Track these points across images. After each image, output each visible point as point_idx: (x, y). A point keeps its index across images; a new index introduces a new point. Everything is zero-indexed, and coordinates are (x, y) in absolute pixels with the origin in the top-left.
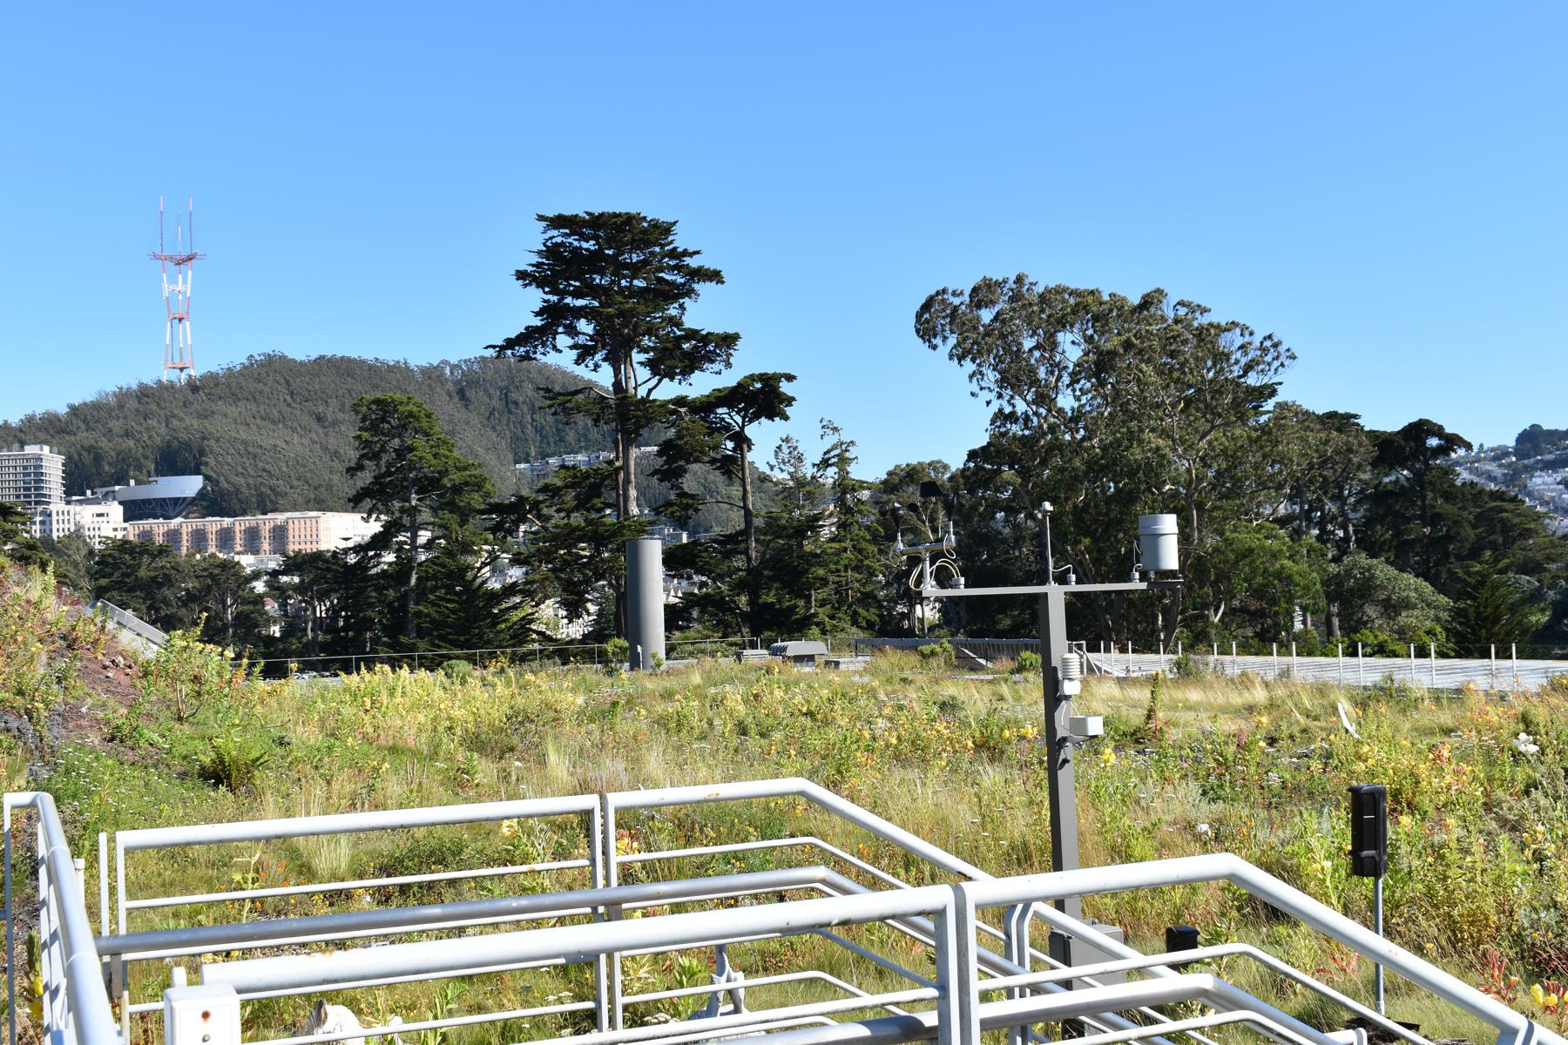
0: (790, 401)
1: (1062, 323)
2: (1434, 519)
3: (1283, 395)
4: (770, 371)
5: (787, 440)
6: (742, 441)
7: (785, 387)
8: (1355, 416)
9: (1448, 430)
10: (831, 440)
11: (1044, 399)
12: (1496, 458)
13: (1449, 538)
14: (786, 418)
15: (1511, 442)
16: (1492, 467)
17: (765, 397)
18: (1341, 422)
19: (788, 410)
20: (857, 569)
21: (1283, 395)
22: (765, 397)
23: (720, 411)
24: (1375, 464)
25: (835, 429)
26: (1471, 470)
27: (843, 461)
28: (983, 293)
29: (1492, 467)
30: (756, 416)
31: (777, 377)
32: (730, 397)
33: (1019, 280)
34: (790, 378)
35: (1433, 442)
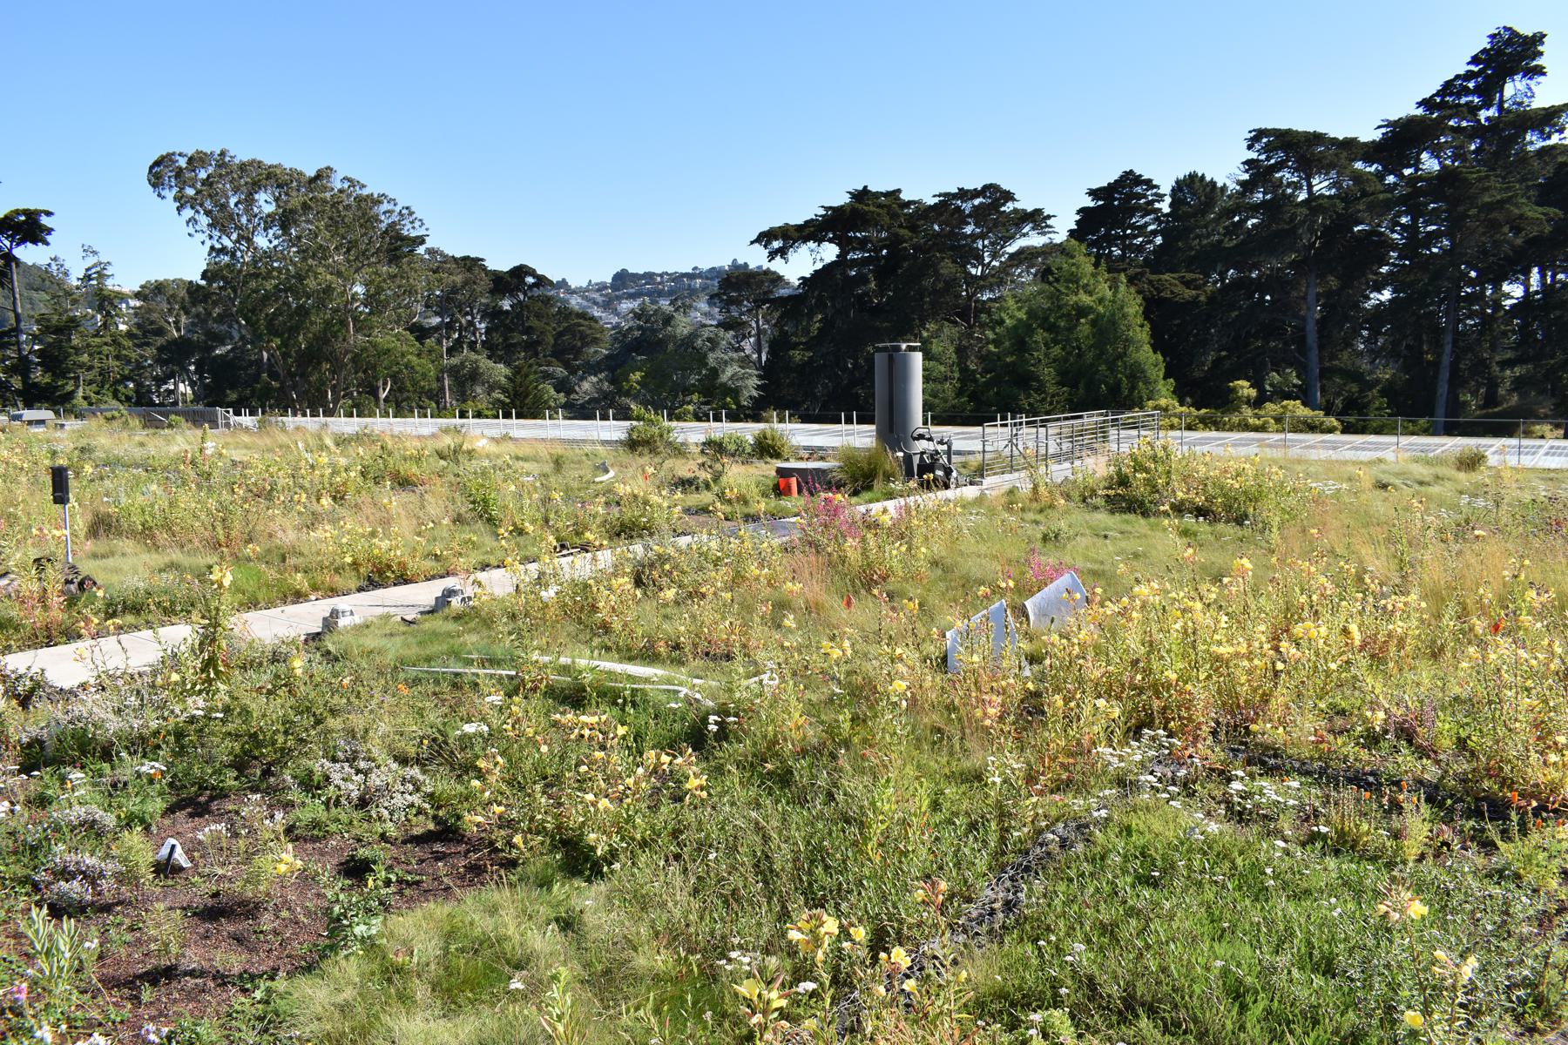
0: (50, 231)
5: (55, 259)
7: (44, 220)
10: (91, 261)
14: (47, 244)
15: (609, 280)
16: (596, 296)
19: (49, 238)
20: (117, 357)
25: (95, 253)
26: (583, 298)
27: (101, 276)
29: (596, 296)
31: (38, 213)
34: (49, 214)
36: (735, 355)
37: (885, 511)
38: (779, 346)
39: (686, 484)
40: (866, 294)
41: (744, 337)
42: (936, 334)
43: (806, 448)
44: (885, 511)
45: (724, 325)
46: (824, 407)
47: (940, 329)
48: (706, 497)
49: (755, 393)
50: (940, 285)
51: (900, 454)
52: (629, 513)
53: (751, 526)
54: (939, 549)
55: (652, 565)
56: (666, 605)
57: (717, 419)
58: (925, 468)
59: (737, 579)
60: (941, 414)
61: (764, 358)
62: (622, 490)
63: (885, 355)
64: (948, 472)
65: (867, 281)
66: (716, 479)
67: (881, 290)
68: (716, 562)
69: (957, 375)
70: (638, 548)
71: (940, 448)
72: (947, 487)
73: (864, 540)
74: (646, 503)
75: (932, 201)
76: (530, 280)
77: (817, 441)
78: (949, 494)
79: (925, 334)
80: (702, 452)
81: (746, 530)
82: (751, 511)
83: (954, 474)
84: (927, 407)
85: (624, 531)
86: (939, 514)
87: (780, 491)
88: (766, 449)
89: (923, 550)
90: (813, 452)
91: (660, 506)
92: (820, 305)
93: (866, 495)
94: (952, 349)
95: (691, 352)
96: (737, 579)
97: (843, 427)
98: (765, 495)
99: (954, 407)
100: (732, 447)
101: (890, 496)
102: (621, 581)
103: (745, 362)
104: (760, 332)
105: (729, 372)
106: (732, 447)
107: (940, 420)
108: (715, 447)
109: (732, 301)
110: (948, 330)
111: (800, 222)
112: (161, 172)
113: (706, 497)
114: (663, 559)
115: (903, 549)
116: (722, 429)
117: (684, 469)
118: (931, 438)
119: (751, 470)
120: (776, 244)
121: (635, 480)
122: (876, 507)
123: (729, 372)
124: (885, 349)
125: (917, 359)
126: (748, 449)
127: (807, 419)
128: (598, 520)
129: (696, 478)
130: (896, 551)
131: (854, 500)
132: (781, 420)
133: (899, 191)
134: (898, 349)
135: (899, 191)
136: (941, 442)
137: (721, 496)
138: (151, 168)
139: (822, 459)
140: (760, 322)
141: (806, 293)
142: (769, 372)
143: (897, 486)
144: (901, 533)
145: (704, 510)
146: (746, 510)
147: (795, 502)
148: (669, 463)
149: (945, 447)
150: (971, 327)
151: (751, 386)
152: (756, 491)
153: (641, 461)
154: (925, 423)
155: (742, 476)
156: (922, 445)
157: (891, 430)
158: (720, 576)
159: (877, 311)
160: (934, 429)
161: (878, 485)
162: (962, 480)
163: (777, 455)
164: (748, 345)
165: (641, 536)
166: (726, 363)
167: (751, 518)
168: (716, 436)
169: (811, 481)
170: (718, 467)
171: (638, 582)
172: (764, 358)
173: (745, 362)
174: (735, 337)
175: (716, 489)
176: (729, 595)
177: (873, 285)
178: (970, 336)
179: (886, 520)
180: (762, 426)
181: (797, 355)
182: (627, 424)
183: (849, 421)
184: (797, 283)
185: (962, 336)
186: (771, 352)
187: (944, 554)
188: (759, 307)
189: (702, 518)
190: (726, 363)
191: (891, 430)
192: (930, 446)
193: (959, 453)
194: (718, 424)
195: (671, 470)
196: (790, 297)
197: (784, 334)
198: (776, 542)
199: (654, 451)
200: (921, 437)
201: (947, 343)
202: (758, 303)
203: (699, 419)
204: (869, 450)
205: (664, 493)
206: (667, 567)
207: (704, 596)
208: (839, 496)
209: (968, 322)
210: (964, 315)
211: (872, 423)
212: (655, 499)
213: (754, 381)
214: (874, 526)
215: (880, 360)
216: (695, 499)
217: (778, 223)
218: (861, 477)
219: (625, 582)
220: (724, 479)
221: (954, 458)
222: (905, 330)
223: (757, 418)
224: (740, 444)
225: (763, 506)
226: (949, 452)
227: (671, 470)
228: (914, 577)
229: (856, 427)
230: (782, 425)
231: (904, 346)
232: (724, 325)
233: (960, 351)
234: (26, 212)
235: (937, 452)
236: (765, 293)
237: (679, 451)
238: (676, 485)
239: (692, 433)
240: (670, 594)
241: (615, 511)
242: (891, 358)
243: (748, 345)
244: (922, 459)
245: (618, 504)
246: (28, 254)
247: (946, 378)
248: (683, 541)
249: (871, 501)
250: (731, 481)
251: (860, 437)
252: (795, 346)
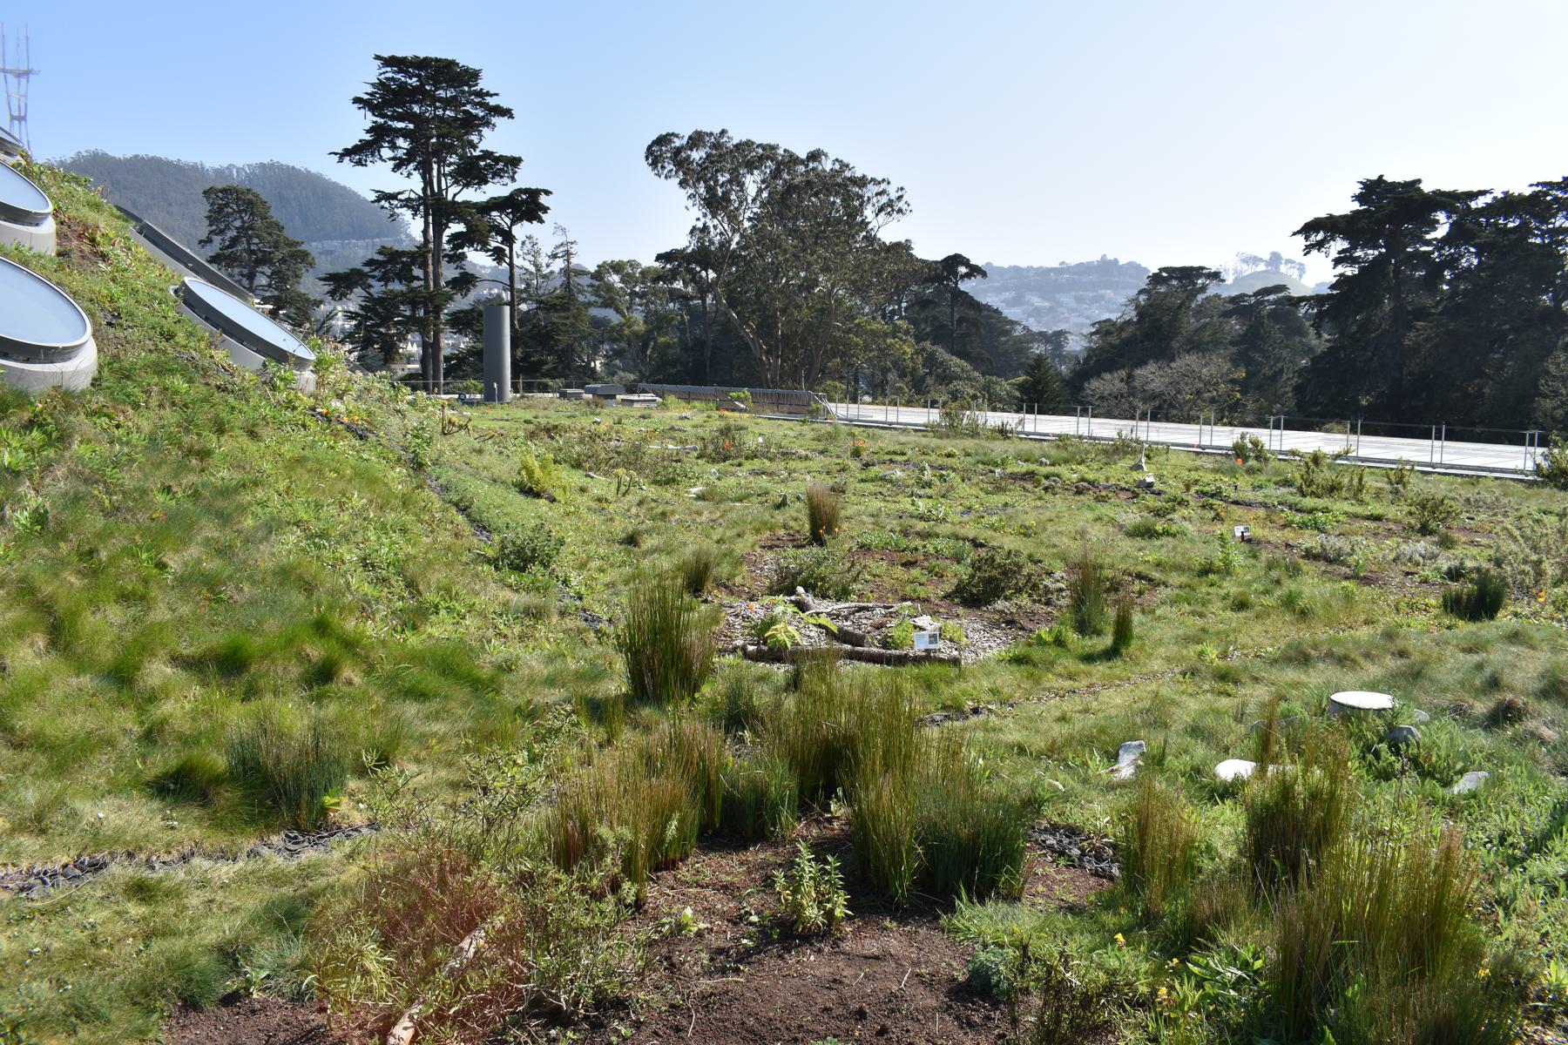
0: (545, 209)
1: (751, 166)
4: (534, 187)
5: (529, 238)
6: (509, 238)
7: (543, 199)
10: (560, 239)
11: (733, 218)
14: (541, 221)
17: (528, 206)
19: (544, 216)
22: (528, 206)
23: (494, 213)
25: (564, 230)
27: (568, 254)
28: (697, 139)
30: (520, 219)
33: (723, 132)
34: (547, 193)
112: (662, 152)
138: (649, 148)
234: (526, 191)
246: (521, 230)
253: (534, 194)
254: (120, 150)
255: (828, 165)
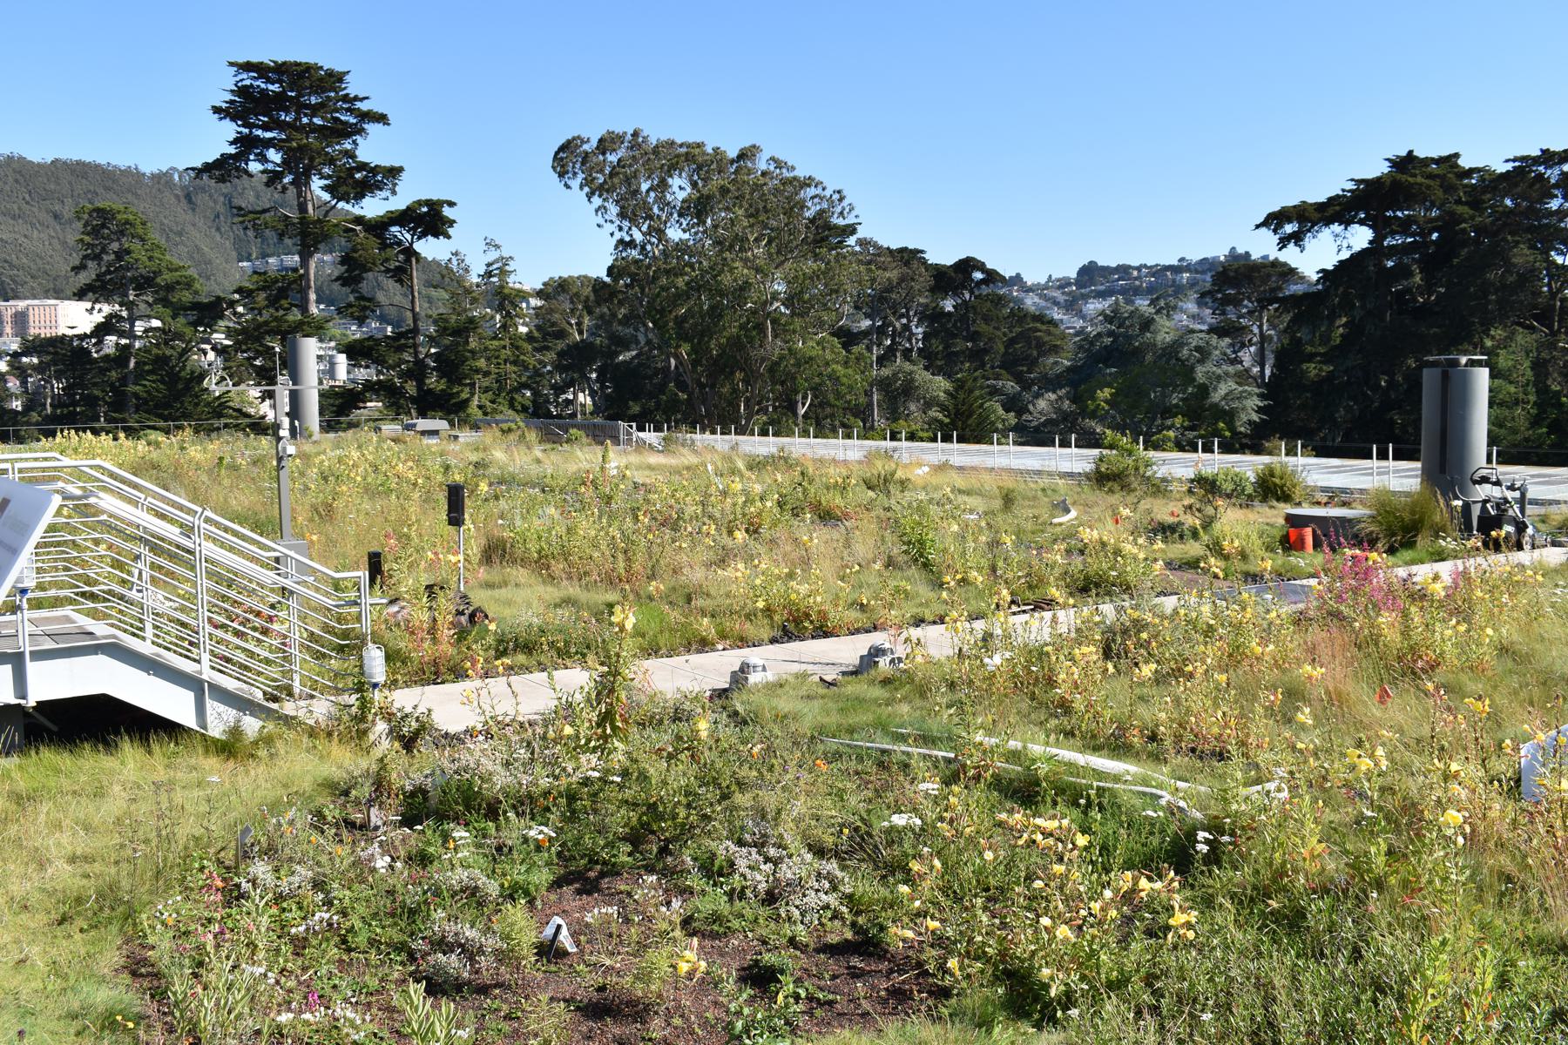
0: (452, 223)
1: (673, 168)
2: (974, 337)
3: (862, 233)
5: (456, 254)
7: (447, 211)
8: (922, 252)
9: (989, 266)
10: (493, 255)
12: (1061, 287)
13: (985, 351)
14: (449, 237)
15: (1074, 275)
16: (1057, 294)
17: (430, 219)
18: (909, 257)
19: (450, 231)
20: (515, 363)
21: (862, 233)
22: (430, 219)
23: (394, 229)
24: (932, 290)
25: (497, 247)
27: (503, 273)
28: (607, 143)
29: (1057, 294)
30: (423, 235)
31: (441, 203)
32: (405, 217)
33: (636, 134)
34: (451, 204)
35: (978, 275)
36: (1231, 369)
37: (1436, 578)
38: (1288, 358)
39: (1167, 531)
40: (1408, 290)
41: (1243, 346)
42: (1504, 344)
43: (1324, 490)
44: (1436, 578)
45: (1219, 331)
46: (1347, 437)
47: (1511, 337)
48: (1193, 549)
49: (1255, 417)
50: (1511, 279)
51: (1459, 503)
52: (1097, 564)
53: (1253, 588)
54: (1508, 632)
55: (1125, 632)
56: (1142, 684)
57: (1208, 449)
58: (1489, 523)
59: (1234, 657)
60: (1510, 451)
61: (1268, 372)
62: (1088, 535)
63: (1437, 371)
64: (1521, 527)
65: (1411, 274)
66: (1208, 524)
67: (1429, 287)
68: (1209, 631)
69: (1532, 398)
70: (1108, 609)
71: (1510, 495)
72: (1520, 547)
73: (1405, 615)
74: (1117, 552)
75: (1502, 168)
76: (978, 275)
77: (1337, 481)
78: (1524, 557)
79: (1489, 343)
80: (1190, 491)
81: (1247, 593)
82: (1252, 568)
83: (1530, 531)
84: (1492, 440)
85: (1087, 587)
86: (1512, 584)
87: (1289, 544)
88: (1271, 489)
89: (1489, 631)
90: (1336, 496)
91: (1135, 558)
92: (1346, 306)
93: (1407, 554)
94: (1527, 364)
95: (1175, 363)
96: (1234, 657)
97: (1374, 463)
98: (1270, 548)
99: (1527, 440)
100: (1228, 487)
101: (1440, 556)
102: (1085, 650)
103: (1243, 377)
104: (1264, 338)
105: (1223, 389)
106: (1228, 487)
107: (1506, 458)
108: (1207, 486)
109: (1227, 301)
110: (1522, 338)
111: (1322, 199)
112: (567, 157)
113: (1193, 549)
114: (1139, 625)
115: (1462, 628)
116: (1215, 463)
117: (1164, 511)
118: (1496, 481)
119: (1251, 515)
120: (1289, 228)
121: (1105, 525)
122: (1423, 572)
123: (1223, 389)
124: (1434, 364)
125: (1482, 377)
126: (1249, 490)
127: (1323, 451)
128: (1057, 572)
129: (1180, 523)
130: (1447, 634)
131: (1391, 560)
132: (1291, 452)
133: (1457, 155)
134: (1456, 363)
135: (1457, 155)
136: (1512, 488)
137: (1216, 549)
138: (557, 153)
139: (1344, 504)
140: (1264, 326)
141: (1326, 290)
142: (1273, 390)
143: (1448, 544)
144: (1458, 606)
145: (1192, 564)
146: (1245, 568)
147: (1308, 559)
148: (1145, 504)
149: (1517, 494)
150: (1554, 334)
151: (1250, 408)
152: (1259, 542)
153: (1114, 499)
154: (1489, 461)
155: (1241, 525)
156: (1484, 491)
157: (1443, 470)
158: (1211, 653)
159: (1423, 313)
160: (1502, 469)
161: (1422, 542)
162: (1540, 540)
163: (1286, 498)
164: (1247, 356)
165: (1109, 593)
166: (1219, 378)
167: (1253, 578)
168: (1208, 471)
169: (1331, 534)
170: (1210, 510)
171: (1107, 653)
172: (1268, 372)
173: (1243, 377)
174: (1232, 345)
175: (1205, 538)
176: (1223, 678)
177: (1418, 279)
178: (1552, 346)
179: (1438, 590)
180: (1266, 459)
181: (1312, 369)
182: (1096, 452)
183: (1383, 456)
184: (1315, 277)
185: (1541, 346)
186: (1279, 364)
187: (1515, 637)
188: (1263, 308)
189: (1188, 575)
190: (1219, 378)
191: (1443, 470)
192: (1496, 492)
193: (1535, 502)
194: (1208, 456)
195: (1149, 512)
196: (1306, 296)
197: (1297, 343)
198: (1286, 610)
199: (1126, 488)
200: (1485, 480)
201: (1520, 356)
202: (1263, 303)
203: (1182, 449)
204: (1407, 494)
205: (1141, 541)
206: (1144, 636)
207: (1191, 676)
208: (1374, 555)
209: (1550, 327)
210: (1544, 317)
211: (1418, 460)
212: (1128, 548)
213: (1254, 402)
214: (1420, 596)
215: (1429, 377)
216: (1179, 550)
217: (1292, 201)
218: (1401, 530)
219: (1091, 652)
220: (1217, 526)
221: (1530, 510)
222: (1461, 334)
223: (1257, 450)
224: (1238, 482)
225: (1269, 564)
226: (1522, 501)
227: (1149, 512)
228: (1475, 669)
229: (1391, 464)
230: (1291, 460)
231: (1464, 360)
232: (1219, 331)
233: (1539, 367)
234: (429, 203)
235: (1506, 501)
236: (1273, 290)
237: (1159, 488)
238: (1155, 531)
239: (1177, 466)
240: (1147, 670)
241: (1078, 561)
242: (1445, 377)
243: (1247, 356)
244: (1484, 509)
245: (1082, 552)
246: (430, 248)
247: (1517, 402)
248: (1169, 603)
249: (1413, 562)
250: (1227, 529)
251: (1399, 477)
252: (1310, 358)
253: (435, 206)
254: (40, 153)
255: (762, 164)
